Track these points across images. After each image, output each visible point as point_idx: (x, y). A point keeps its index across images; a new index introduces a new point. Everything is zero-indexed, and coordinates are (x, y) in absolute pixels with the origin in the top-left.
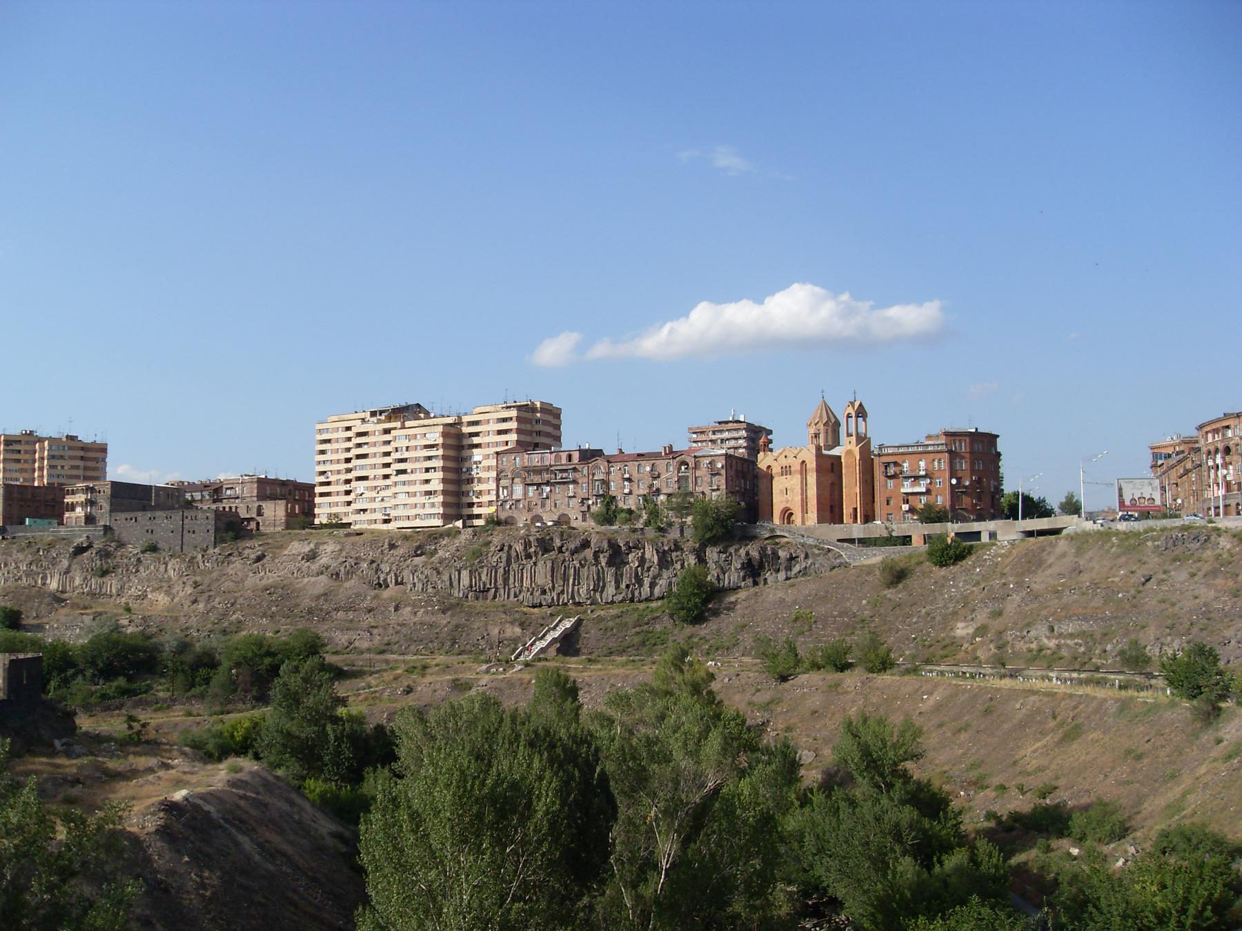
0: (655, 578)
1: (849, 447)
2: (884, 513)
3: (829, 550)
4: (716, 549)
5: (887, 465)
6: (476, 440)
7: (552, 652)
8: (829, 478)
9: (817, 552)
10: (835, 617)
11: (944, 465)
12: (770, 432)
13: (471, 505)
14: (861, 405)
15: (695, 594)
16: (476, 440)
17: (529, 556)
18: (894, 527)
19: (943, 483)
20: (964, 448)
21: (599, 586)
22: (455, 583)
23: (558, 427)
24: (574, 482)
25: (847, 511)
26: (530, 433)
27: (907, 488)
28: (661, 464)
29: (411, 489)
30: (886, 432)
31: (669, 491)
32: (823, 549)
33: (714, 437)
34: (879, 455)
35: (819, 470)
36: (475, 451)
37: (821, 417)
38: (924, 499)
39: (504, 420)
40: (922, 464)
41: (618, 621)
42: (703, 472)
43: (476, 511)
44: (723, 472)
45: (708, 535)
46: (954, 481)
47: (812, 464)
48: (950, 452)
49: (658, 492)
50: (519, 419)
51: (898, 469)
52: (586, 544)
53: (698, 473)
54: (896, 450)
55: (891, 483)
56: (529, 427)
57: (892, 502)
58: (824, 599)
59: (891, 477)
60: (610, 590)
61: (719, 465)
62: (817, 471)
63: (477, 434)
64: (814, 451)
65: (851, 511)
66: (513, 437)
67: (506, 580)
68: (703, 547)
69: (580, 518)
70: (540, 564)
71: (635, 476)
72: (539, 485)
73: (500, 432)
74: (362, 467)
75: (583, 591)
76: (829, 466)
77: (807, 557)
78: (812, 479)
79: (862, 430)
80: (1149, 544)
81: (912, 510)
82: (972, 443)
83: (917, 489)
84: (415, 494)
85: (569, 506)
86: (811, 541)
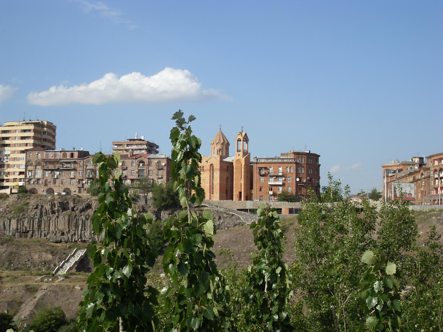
1: (238, 158)
2: (258, 195)
3: (233, 215)
4: (167, 212)
5: (260, 169)
6: (7, 142)
7: (74, 270)
8: (226, 174)
9: (225, 216)
10: (245, 253)
11: (293, 170)
12: (158, 147)
13: (3, 180)
14: (246, 134)
15: (159, 238)
16: (7, 142)
17: (53, 212)
18: (272, 203)
19: (292, 180)
20: (303, 161)
22: (7, 227)
23: (54, 137)
24: (75, 170)
25: (235, 194)
26: (40, 139)
27: (272, 182)
30: (259, 151)
31: (133, 177)
32: (229, 214)
33: (127, 148)
34: (257, 163)
35: (221, 170)
36: (6, 148)
37: (220, 140)
38: (281, 188)
39: (25, 131)
40: (281, 169)
42: (153, 167)
43: (5, 184)
44: (165, 168)
45: (163, 204)
46: (298, 180)
47: (217, 166)
48: (296, 163)
50: (35, 131)
51: (267, 171)
52: (89, 206)
53: (150, 168)
54: (266, 161)
55: (262, 179)
56: (39, 136)
57: (263, 190)
58: (236, 242)
59: (263, 176)
61: (163, 164)
62: (220, 170)
63: (7, 138)
64: (219, 159)
65: (238, 193)
66: (32, 141)
67: (39, 226)
68: (160, 210)
69: (77, 191)
70: (61, 217)
72: (52, 170)
73: (23, 138)
75: (87, 234)
76: (226, 168)
77: (220, 218)
78: (217, 175)
79: (246, 148)
80: (434, 218)
81: (274, 195)
82: (308, 158)
83: (277, 183)
85: (72, 183)
86: (222, 210)
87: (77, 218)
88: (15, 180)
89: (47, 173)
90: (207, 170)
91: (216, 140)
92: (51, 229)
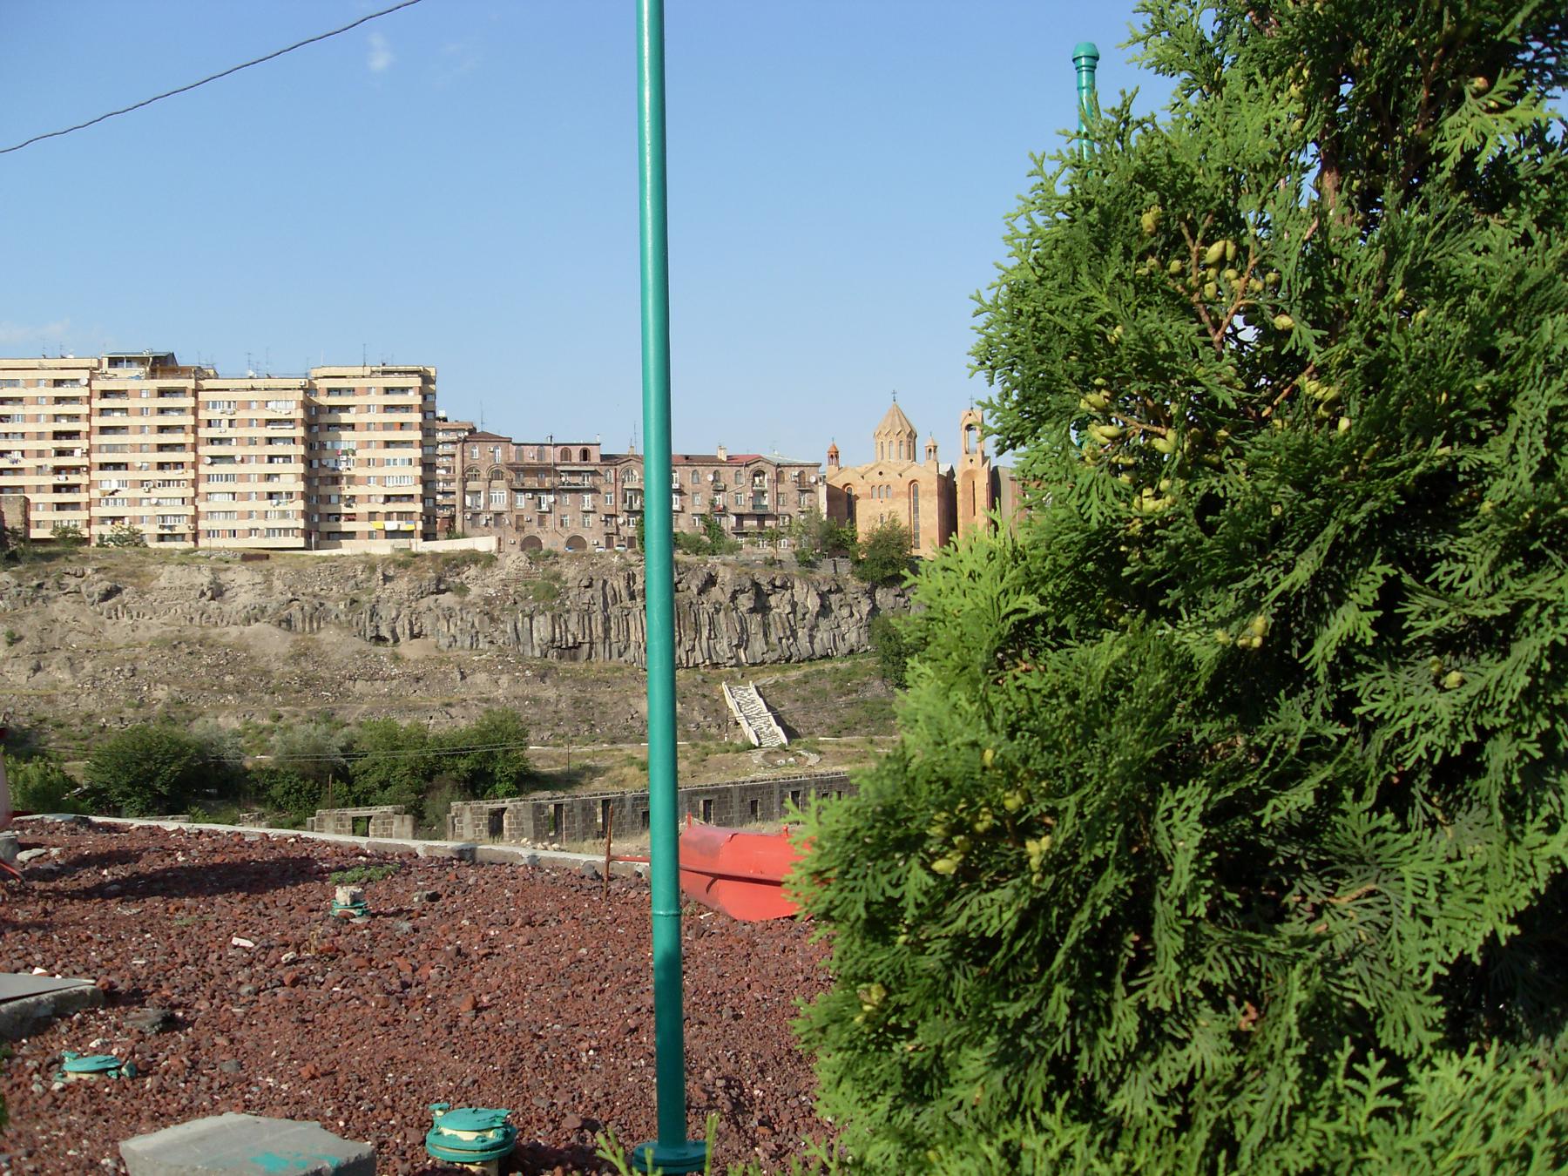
0: (812, 629)
1: (970, 466)
6: (345, 418)
13: (338, 516)
16: (345, 418)
21: (743, 643)
22: (524, 637)
24: (594, 490)
28: (728, 473)
29: (240, 487)
36: (346, 435)
41: (808, 687)
49: (723, 512)
60: (758, 645)
63: (346, 408)
67: (607, 631)
68: (874, 588)
69: (603, 543)
71: (688, 487)
72: (534, 491)
74: (112, 448)
75: (723, 647)
84: (247, 496)
87: (695, 607)
88: (372, 516)
89: (522, 500)
90: (898, 494)
91: (893, 425)
92: (633, 638)
